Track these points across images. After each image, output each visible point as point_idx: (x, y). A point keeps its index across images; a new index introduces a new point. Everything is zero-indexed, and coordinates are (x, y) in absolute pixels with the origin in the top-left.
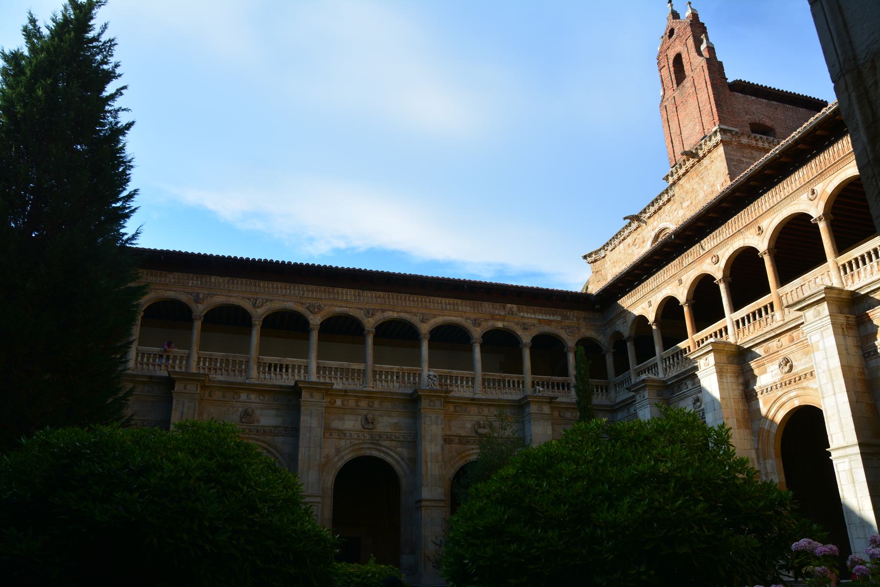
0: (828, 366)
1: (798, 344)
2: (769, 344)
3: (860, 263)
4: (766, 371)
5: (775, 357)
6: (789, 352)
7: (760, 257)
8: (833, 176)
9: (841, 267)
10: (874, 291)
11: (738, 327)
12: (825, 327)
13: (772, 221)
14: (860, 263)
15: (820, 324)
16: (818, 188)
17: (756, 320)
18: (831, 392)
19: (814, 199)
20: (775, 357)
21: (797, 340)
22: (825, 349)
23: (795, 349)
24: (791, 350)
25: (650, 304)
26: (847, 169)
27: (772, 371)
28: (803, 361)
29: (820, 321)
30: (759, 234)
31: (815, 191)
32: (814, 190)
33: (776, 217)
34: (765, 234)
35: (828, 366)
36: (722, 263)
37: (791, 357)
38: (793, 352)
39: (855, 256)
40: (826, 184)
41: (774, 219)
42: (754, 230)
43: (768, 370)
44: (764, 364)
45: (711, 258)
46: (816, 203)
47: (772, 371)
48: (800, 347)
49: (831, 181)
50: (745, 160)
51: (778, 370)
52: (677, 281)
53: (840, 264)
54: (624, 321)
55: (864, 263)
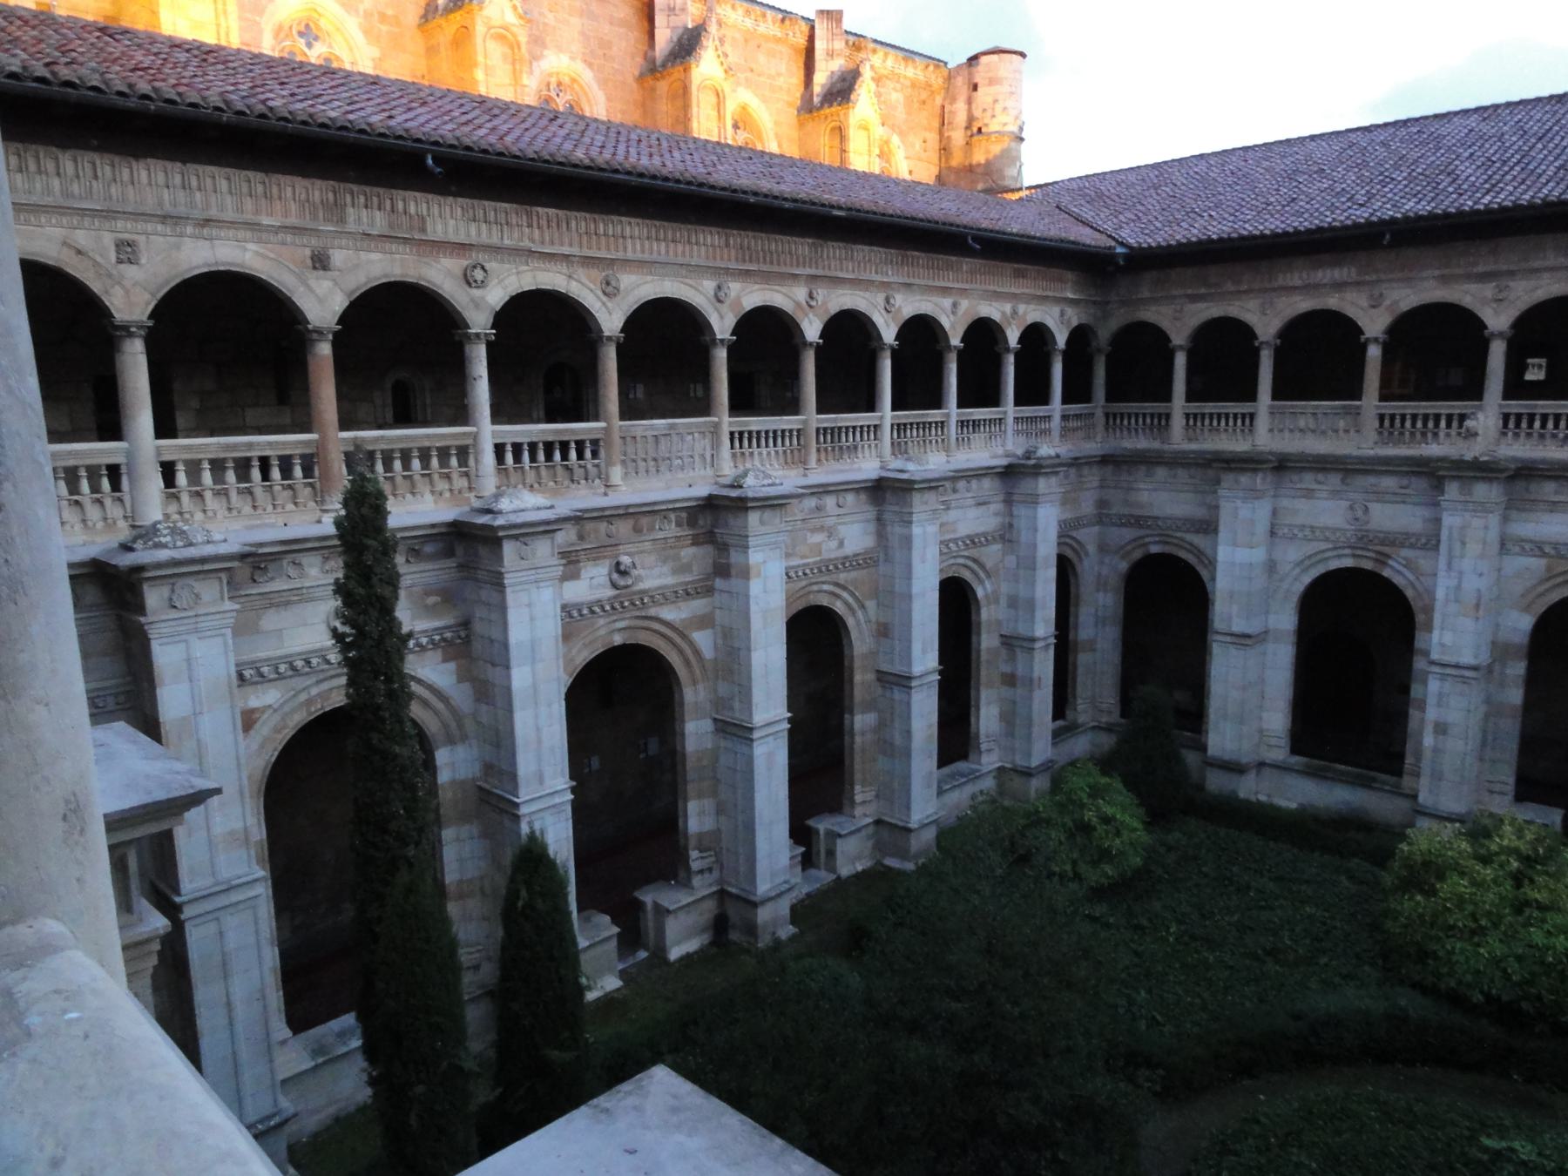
16: (734, 287)
25: (127, 251)
27: (592, 578)
28: (656, 571)
36: (496, 295)
42: (598, 274)
43: (584, 574)
44: (578, 561)
47: (592, 578)
52: (308, 252)
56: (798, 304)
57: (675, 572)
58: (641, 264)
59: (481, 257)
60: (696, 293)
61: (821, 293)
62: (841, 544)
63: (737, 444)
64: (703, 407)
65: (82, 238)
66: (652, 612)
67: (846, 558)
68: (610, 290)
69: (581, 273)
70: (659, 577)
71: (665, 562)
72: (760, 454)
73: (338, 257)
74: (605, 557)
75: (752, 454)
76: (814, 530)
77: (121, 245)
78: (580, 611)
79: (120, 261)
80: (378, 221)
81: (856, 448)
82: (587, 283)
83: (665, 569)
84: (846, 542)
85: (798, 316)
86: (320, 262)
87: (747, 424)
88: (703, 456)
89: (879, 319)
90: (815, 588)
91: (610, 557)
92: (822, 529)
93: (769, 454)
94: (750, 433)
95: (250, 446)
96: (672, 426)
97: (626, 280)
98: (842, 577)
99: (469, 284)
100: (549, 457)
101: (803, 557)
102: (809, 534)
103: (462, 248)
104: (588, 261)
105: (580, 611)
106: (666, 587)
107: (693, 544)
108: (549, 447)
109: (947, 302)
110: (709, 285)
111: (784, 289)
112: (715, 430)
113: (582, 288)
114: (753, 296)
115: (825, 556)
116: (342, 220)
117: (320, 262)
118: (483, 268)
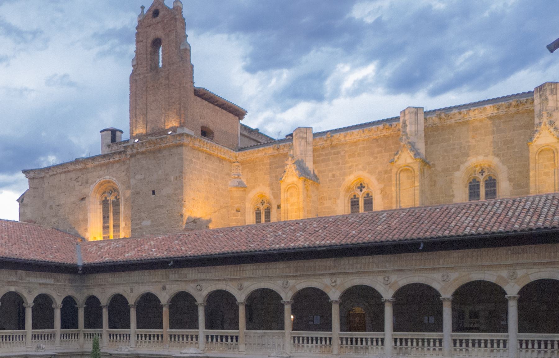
3: (305, 341)
7: (237, 304)
11: (207, 340)
13: (252, 285)
14: (305, 341)
16: (292, 282)
25: (132, 290)
33: (255, 284)
36: (205, 293)
39: (303, 336)
41: (254, 284)
45: (197, 285)
49: (301, 283)
50: (194, 160)
52: (162, 286)
54: (103, 292)
58: (251, 278)
59: (199, 283)
60: (275, 286)
61: (339, 280)
63: (296, 341)
65: (125, 288)
72: (307, 346)
73: (167, 287)
75: (303, 346)
77: (131, 289)
79: (131, 292)
80: (176, 276)
81: (367, 348)
85: (326, 291)
86: (164, 288)
87: (300, 334)
88: (279, 345)
89: (380, 288)
93: (312, 347)
95: (151, 332)
96: (265, 333)
97: (246, 284)
99: (201, 290)
100: (222, 340)
103: (195, 281)
104: (232, 280)
108: (222, 337)
109: (437, 276)
110: (280, 282)
112: (283, 335)
113: (232, 288)
114: (302, 284)
116: (169, 278)
117: (164, 288)
118: (200, 285)
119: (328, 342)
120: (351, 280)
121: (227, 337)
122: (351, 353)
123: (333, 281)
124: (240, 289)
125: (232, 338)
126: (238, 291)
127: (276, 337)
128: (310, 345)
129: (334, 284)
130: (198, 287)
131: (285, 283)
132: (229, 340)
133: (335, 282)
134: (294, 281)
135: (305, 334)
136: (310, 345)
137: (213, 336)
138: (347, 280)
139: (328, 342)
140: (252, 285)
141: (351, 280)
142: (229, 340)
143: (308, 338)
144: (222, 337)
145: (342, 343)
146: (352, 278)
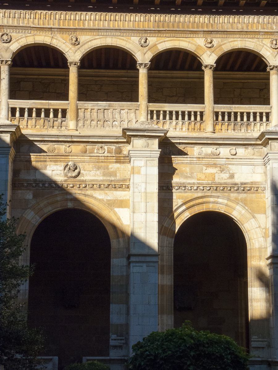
0: (146, 189)
1: (93, 158)
2: (55, 145)
4: (46, 169)
5: (61, 160)
6: (80, 160)
8: (168, 39)
9: (149, 112)
10: (180, 143)
12: (152, 158)
13: (92, 40)
15: (150, 155)
16: (152, 40)
17: (32, 116)
18: (143, 210)
19: (145, 47)
20: (61, 160)
21: (90, 153)
22: (146, 175)
23: (88, 160)
24: (83, 160)
26: (182, 40)
27: (53, 171)
28: (93, 173)
29: (150, 152)
30: (75, 44)
31: (147, 41)
32: (147, 39)
34: (81, 47)
35: (146, 189)
37: (80, 165)
38: (84, 162)
39: (165, 109)
40: (160, 41)
41: (95, 39)
42: (67, 36)
44: (45, 161)
46: (145, 51)
47: (53, 171)
48: (94, 160)
49: (165, 41)
51: (62, 172)
53: (150, 109)
55: (171, 118)
56: (199, 47)
57: (104, 175)
59: (8, 31)
62: (232, 176)
64: (133, 97)
66: (89, 192)
67: (236, 184)
68: (76, 43)
69: (58, 36)
70: (94, 176)
71: (99, 168)
74: (61, 161)
76: (208, 165)
78: (43, 184)
82: (61, 39)
83: (98, 172)
84: (236, 176)
85: (198, 53)
90: (212, 199)
91: (64, 161)
92: (215, 165)
94: (165, 112)
97: (83, 38)
98: (233, 195)
101: (198, 180)
102: (204, 168)
104: (61, 30)
105: (43, 184)
106: (97, 180)
107: (116, 162)
108: (39, 112)
111: (188, 40)
115: (217, 180)
119: (199, 118)
120: (231, 42)
121: (47, 112)
122: (229, 131)
123: (209, 41)
124: (74, 44)
125: (56, 111)
126: (71, 46)
127: (126, 110)
128: (174, 122)
129: (210, 45)
130: (5, 37)
131: (143, 41)
132: (51, 115)
133: (211, 43)
134: (154, 39)
135: (168, 107)
136: (174, 122)
137: (24, 109)
138: (225, 42)
139: (199, 118)
140: (92, 40)
141: (231, 42)
142: (51, 115)
143: (171, 113)
144: (39, 112)
145: (217, 119)
146: (232, 39)
